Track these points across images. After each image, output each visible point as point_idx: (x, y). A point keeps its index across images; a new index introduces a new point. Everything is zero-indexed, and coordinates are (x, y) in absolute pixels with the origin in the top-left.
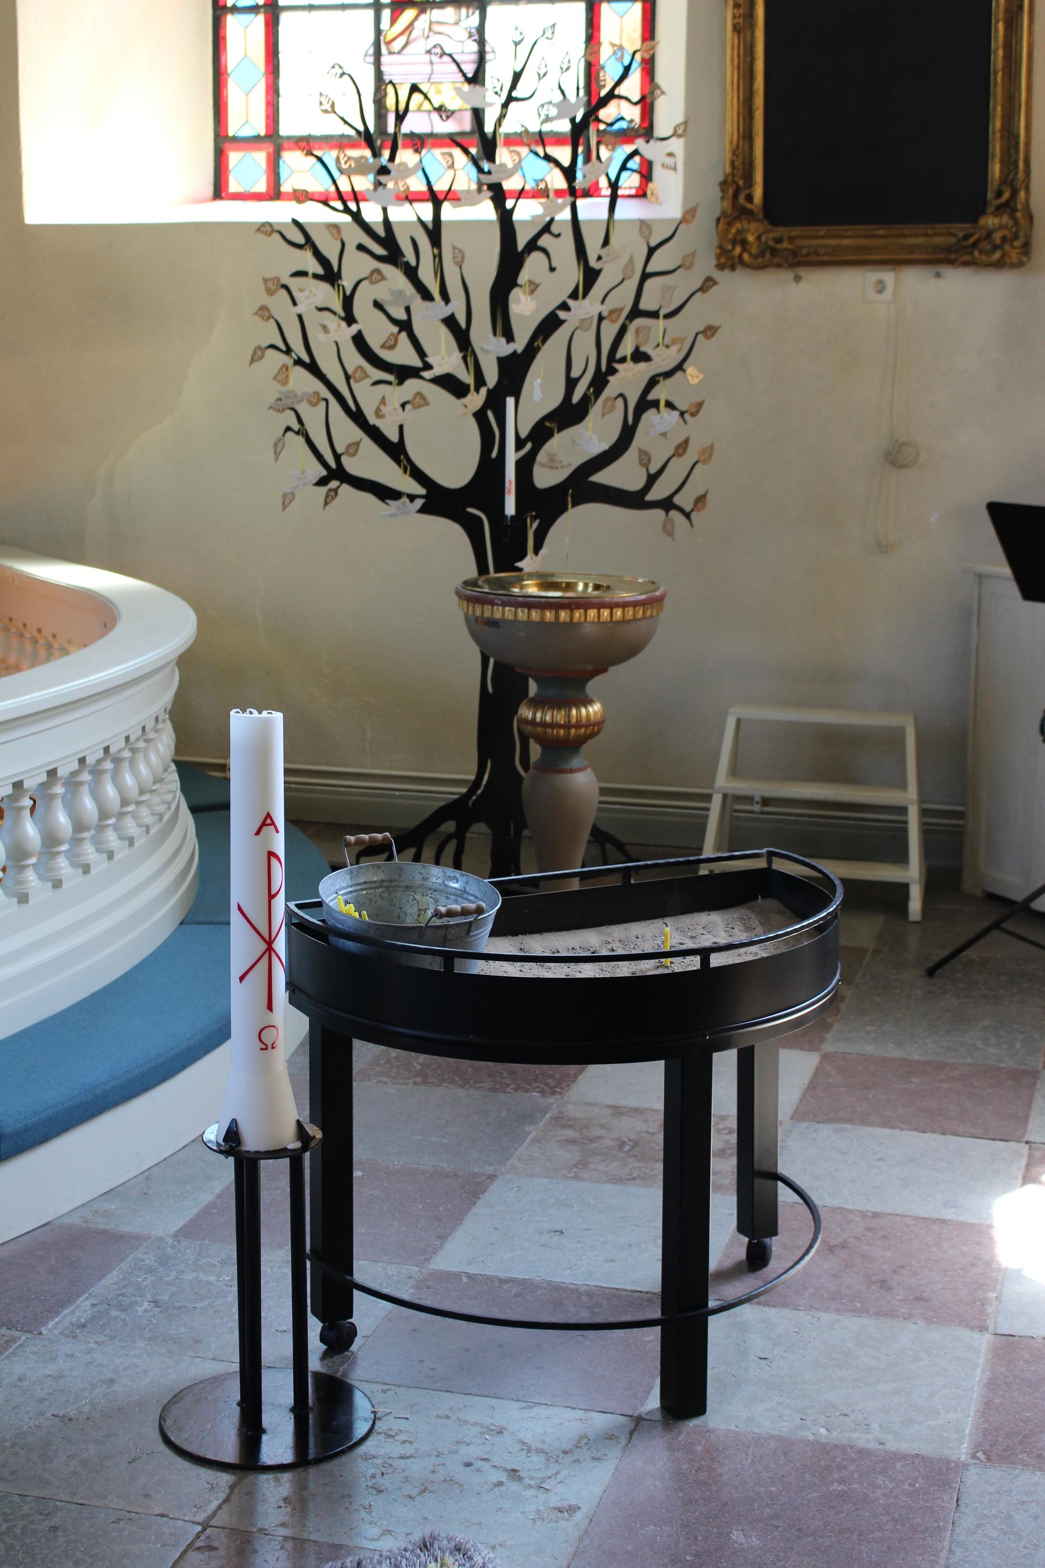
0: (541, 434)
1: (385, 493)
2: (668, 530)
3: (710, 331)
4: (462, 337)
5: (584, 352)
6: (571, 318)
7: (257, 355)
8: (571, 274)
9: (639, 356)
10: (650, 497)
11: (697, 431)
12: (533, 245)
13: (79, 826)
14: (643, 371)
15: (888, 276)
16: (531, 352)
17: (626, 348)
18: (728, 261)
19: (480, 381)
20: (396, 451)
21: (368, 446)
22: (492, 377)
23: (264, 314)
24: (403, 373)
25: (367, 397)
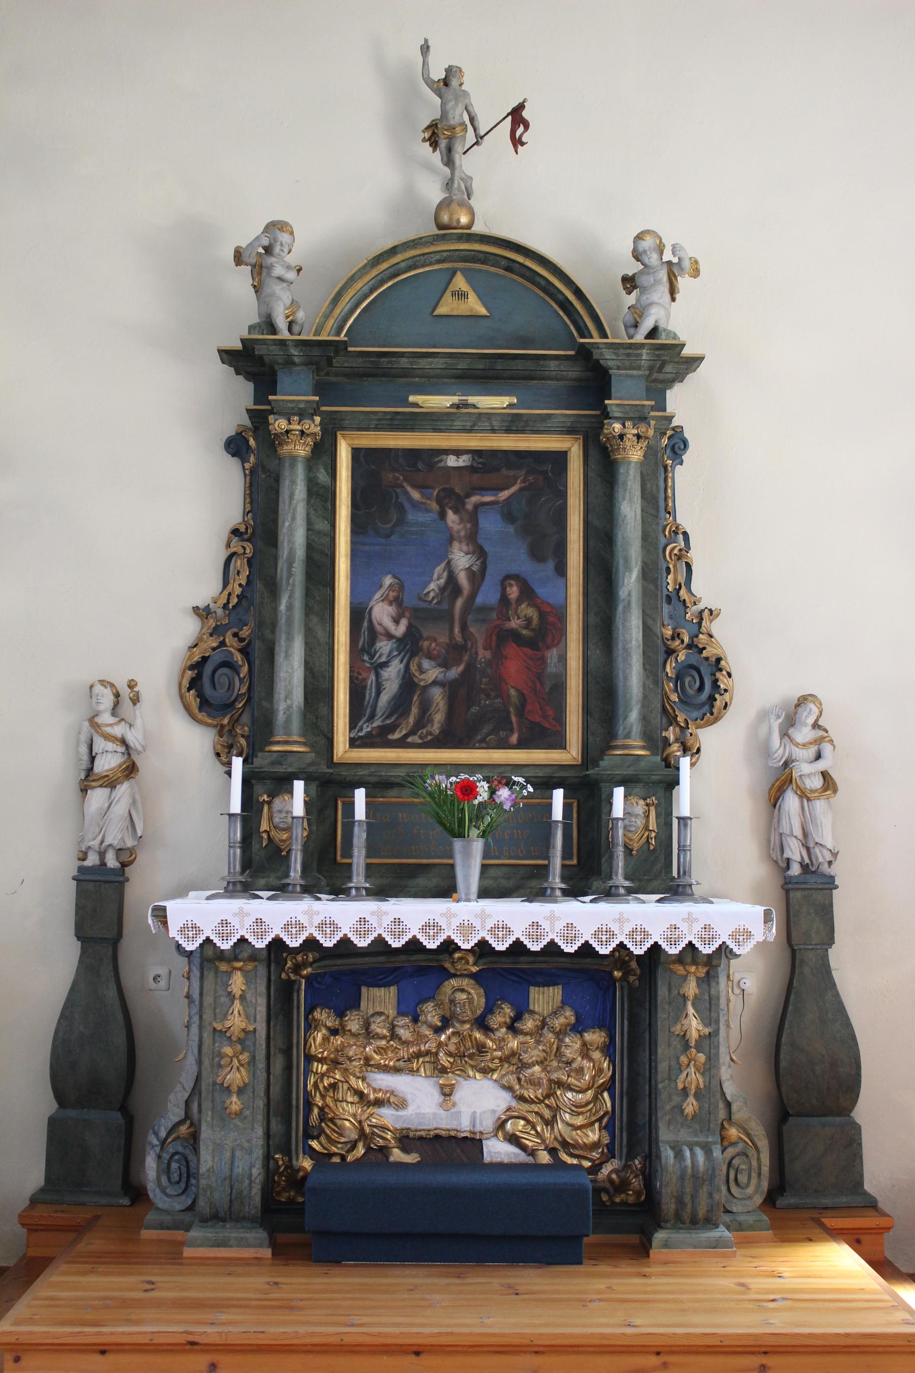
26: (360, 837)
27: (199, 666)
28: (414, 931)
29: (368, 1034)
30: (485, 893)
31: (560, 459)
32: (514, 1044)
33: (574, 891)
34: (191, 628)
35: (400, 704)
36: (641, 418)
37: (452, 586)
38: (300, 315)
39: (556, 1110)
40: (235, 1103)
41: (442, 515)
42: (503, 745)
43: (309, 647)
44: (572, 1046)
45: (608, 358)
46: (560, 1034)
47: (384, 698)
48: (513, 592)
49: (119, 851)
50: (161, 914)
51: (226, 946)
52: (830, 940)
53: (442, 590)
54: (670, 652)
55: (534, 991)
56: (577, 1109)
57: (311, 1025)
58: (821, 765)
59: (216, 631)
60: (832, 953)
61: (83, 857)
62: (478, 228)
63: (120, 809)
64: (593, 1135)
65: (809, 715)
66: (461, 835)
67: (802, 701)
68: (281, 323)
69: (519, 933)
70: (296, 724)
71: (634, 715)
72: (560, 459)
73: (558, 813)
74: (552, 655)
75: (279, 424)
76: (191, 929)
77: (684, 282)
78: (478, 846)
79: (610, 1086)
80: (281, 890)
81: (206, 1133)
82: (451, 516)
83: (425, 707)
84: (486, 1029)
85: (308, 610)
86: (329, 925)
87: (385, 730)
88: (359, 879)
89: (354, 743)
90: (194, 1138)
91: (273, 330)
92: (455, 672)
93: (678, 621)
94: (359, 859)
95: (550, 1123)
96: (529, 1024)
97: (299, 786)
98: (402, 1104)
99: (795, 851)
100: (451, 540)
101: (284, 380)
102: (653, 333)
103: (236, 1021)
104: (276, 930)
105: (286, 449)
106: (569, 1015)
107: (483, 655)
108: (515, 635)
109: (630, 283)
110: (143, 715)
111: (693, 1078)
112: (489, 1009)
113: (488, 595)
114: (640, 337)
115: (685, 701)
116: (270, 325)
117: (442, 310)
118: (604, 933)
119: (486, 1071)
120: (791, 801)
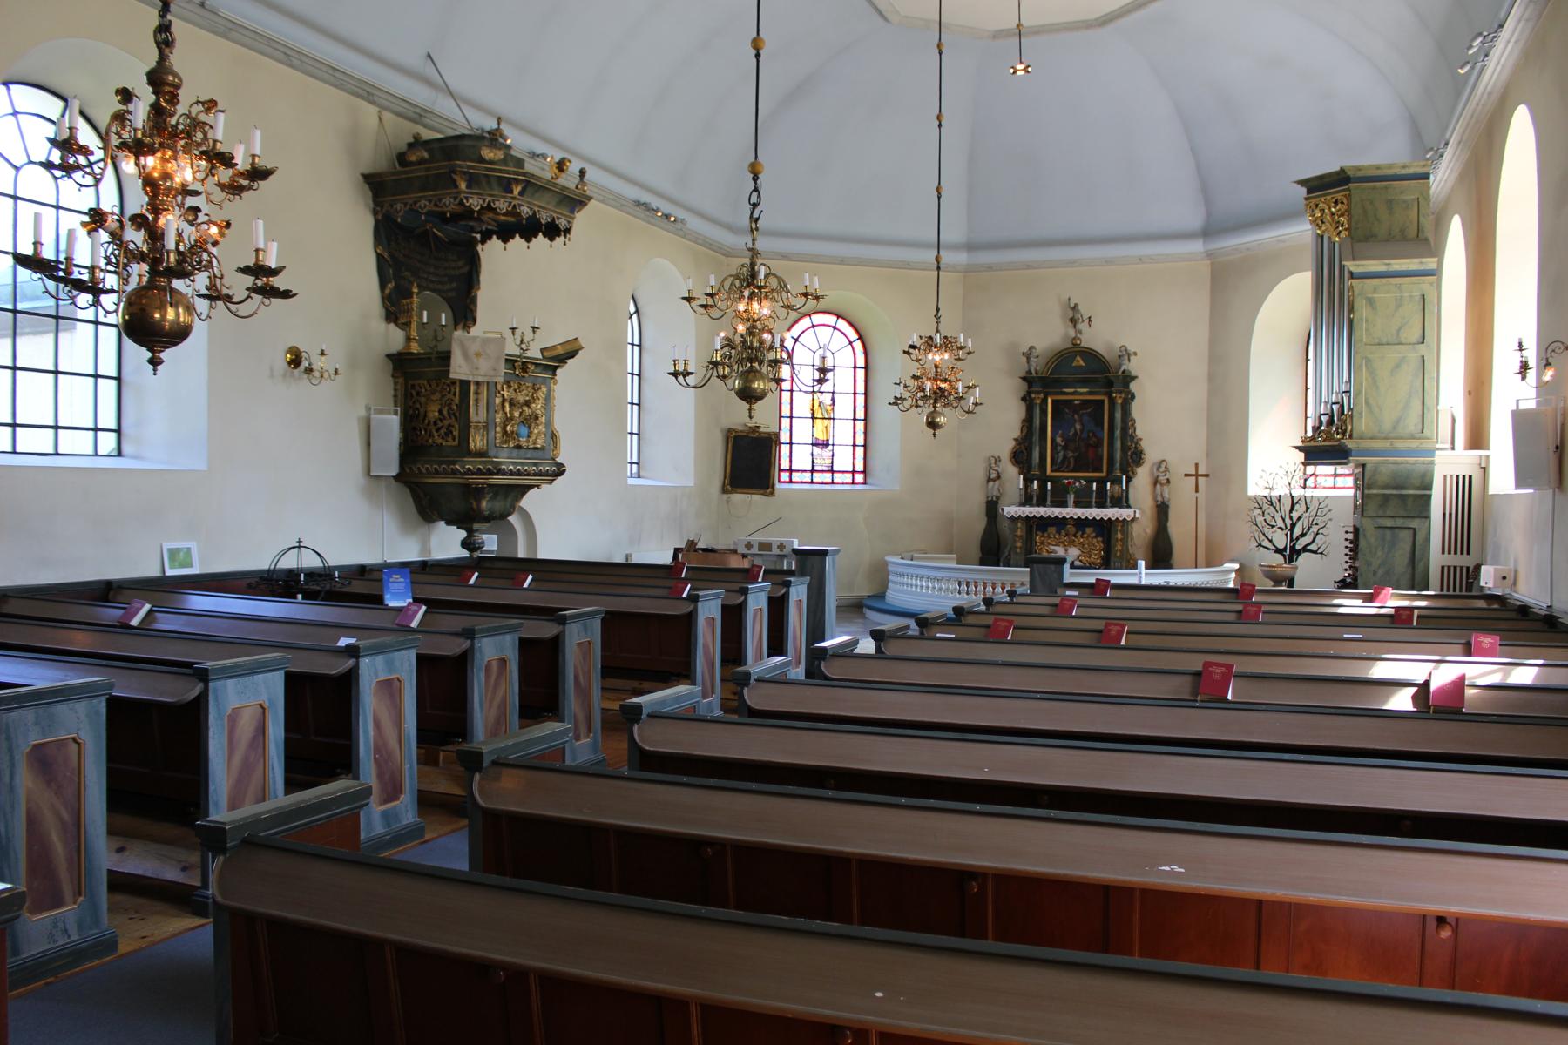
0: (1297, 539)
1: (1268, 549)
2: (1322, 558)
3: (1330, 520)
4: (1284, 520)
5: (1306, 525)
6: (1303, 517)
7: (1247, 522)
8: (1304, 509)
9: (1316, 524)
10: (1319, 551)
12: (1297, 503)
14: (1318, 527)
17: (1314, 523)
19: (1286, 528)
20: (1271, 541)
21: (1266, 540)
22: (1289, 528)
24: (1273, 526)
26: (1049, 494)
27: (1016, 451)
28: (1056, 514)
31: (1103, 401)
32: (1082, 540)
34: (1014, 443)
35: (1063, 462)
36: (1120, 392)
37: (1076, 433)
38: (1038, 368)
40: (1019, 550)
41: (1073, 416)
42: (1088, 472)
43: (1040, 448)
44: (1095, 540)
45: (1112, 378)
46: (1092, 538)
47: (1059, 460)
48: (1091, 435)
50: (1002, 509)
53: (1073, 435)
54: (1130, 449)
56: (1095, 555)
57: (1037, 535)
58: (1167, 477)
59: (1019, 444)
60: (1169, 524)
61: (988, 497)
62: (1082, 345)
63: (996, 486)
64: (1099, 561)
65: (1164, 464)
67: (1163, 461)
68: (1033, 372)
69: (1079, 515)
71: (1118, 465)
72: (1103, 401)
75: (1033, 396)
76: (1009, 513)
77: (1132, 358)
78: (1073, 496)
79: (1103, 550)
80: (1031, 505)
81: (1012, 556)
82: (1076, 416)
83: (1069, 463)
85: (1040, 440)
86: (1038, 512)
87: (1059, 468)
88: (1048, 503)
89: (1052, 471)
90: (1010, 560)
91: (1031, 374)
92: (1076, 454)
93: (1132, 441)
95: (1090, 557)
96: (1085, 536)
97: (1036, 482)
98: (1056, 553)
99: (1159, 499)
100: (1075, 421)
102: (1124, 372)
103: (1019, 533)
104: (1027, 513)
105: (1035, 401)
106: (1094, 534)
109: (1120, 356)
110: (1002, 465)
111: (1119, 547)
112: (1077, 532)
113: (1085, 435)
114: (1120, 373)
115: (1133, 461)
117: (1074, 365)
118: (1098, 515)
119: (1075, 546)
120: (1158, 486)
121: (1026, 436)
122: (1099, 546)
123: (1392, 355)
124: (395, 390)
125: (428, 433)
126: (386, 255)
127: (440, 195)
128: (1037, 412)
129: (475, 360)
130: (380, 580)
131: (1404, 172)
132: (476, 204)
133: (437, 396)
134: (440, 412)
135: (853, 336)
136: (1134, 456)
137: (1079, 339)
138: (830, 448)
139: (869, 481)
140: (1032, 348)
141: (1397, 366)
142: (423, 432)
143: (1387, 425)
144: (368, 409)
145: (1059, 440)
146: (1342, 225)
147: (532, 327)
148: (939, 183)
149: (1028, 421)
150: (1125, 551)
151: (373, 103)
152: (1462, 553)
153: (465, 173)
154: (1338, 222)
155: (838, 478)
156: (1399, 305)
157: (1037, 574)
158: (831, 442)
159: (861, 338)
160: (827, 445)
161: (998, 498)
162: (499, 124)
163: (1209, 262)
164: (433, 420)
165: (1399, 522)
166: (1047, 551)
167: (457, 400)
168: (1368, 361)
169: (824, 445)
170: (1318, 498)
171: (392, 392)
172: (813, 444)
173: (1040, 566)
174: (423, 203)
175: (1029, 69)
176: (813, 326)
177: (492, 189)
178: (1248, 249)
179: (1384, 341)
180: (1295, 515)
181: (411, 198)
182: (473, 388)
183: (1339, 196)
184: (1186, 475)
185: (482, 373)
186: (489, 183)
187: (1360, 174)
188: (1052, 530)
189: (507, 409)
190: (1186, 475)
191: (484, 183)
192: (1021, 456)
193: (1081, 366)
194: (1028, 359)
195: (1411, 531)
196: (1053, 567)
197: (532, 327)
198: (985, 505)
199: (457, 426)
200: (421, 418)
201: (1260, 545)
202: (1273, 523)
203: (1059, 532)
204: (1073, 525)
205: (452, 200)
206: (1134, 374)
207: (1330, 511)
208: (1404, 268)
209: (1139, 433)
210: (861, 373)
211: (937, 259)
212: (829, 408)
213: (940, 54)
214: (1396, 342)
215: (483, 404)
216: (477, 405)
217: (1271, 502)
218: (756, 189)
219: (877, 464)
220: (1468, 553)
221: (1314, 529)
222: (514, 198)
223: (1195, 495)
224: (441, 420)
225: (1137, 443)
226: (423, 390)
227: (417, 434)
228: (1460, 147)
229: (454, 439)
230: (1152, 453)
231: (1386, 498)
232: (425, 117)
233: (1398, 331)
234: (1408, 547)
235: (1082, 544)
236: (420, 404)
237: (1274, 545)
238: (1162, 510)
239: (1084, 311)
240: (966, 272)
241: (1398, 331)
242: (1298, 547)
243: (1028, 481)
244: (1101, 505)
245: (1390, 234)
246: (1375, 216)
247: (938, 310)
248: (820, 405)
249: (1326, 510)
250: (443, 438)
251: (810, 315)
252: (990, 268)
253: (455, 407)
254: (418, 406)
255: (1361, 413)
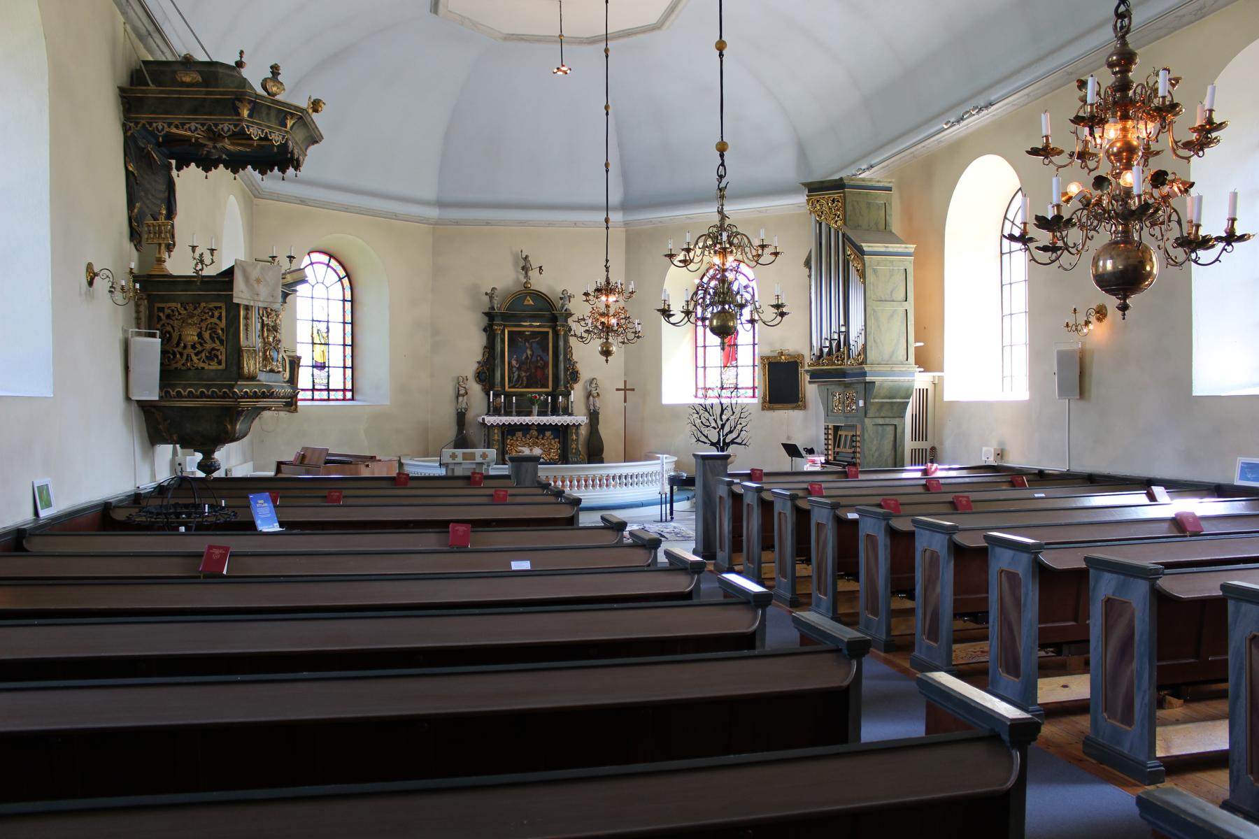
0: (727, 435)
1: (705, 443)
3: (751, 420)
4: (716, 422)
9: (740, 424)
11: (749, 434)
13: (656, 479)
14: (741, 426)
15: (787, 411)
16: (725, 423)
18: (763, 409)
20: (707, 437)
22: (720, 427)
23: (689, 418)
24: (708, 426)
25: (702, 429)
27: (479, 373)
29: (517, 440)
30: (538, 415)
31: (548, 332)
33: (553, 415)
34: (476, 366)
35: (517, 381)
36: (563, 326)
37: (527, 358)
39: (550, 453)
42: (537, 388)
43: (501, 370)
44: (553, 442)
45: (558, 315)
47: (514, 379)
48: (539, 358)
49: (465, 409)
51: (495, 424)
52: (598, 424)
55: (546, 433)
57: (507, 439)
58: (597, 391)
59: (482, 366)
62: (531, 288)
65: (595, 381)
66: (534, 405)
67: (593, 379)
70: (499, 384)
71: (562, 383)
72: (548, 332)
73: (550, 401)
74: (546, 371)
75: (496, 327)
76: (489, 421)
77: (571, 299)
78: (537, 407)
80: (500, 415)
82: (527, 344)
84: (538, 439)
87: (515, 385)
88: (514, 413)
89: (509, 388)
91: (494, 310)
92: (528, 374)
94: (514, 409)
97: (503, 396)
99: (592, 407)
100: (527, 348)
101: (496, 319)
102: (566, 310)
103: (496, 437)
104: (504, 422)
107: (533, 371)
108: (539, 367)
109: (561, 299)
111: (574, 446)
112: (538, 436)
113: (534, 359)
115: (571, 379)
116: (493, 308)
117: (525, 303)
119: (538, 447)
120: (591, 398)
121: (487, 359)
122: (557, 445)
123: (889, 307)
124: (138, 312)
125: (185, 357)
126: (136, 173)
127: (152, 118)
128: (498, 340)
129: (256, 285)
130: (248, 507)
131: (878, 184)
132: (255, 134)
133: (195, 320)
134: (200, 335)
135: (342, 273)
136: (573, 376)
137: (530, 283)
138: (327, 369)
139: (356, 397)
140: (493, 289)
141: (892, 316)
142: (178, 356)
143: (886, 357)
144: (125, 331)
145: (514, 363)
146: (838, 217)
147: (288, 257)
148: (607, 160)
149: (490, 348)
150: (577, 449)
151: (124, 13)
152: (919, 440)
153: (250, 101)
154: (836, 215)
155: (333, 395)
156: (891, 275)
157: (708, 467)
158: (327, 365)
159: (348, 275)
160: (324, 367)
161: (466, 410)
162: (241, 57)
163: (624, 229)
164: (189, 344)
165: (887, 421)
166: (516, 452)
167: (223, 324)
168: (875, 311)
169: (322, 367)
170: (741, 405)
171: (134, 315)
172: (313, 367)
173: (711, 461)
174: (193, 125)
175: (555, 70)
176: (312, 264)
177: (269, 121)
178: (660, 222)
179: (883, 298)
180: (724, 417)
181: (178, 119)
182: (242, 313)
183: (836, 196)
184: (617, 390)
185: (262, 299)
186: (268, 114)
187: (852, 183)
188: (519, 434)
189: (266, 334)
190: (617, 390)
191: (264, 114)
192: (485, 375)
193: (531, 305)
194: (491, 298)
195: (893, 427)
196: (719, 462)
197: (288, 257)
198: (456, 416)
199: (223, 349)
200: (175, 341)
201: (698, 440)
202: (708, 424)
203: (524, 435)
204: (536, 430)
205: (232, 127)
206: (573, 312)
207: (750, 414)
208: (895, 250)
209: (575, 358)
210: (348, 305)
211: (607, 220)
212: (325, 335)
213: (607, 57)
214: (891, 299)
215: (256, 325)
216: (247, 330)
217: (706, 408)
218: (722, 164)
219: (363, 383)
220: (926, 440)
221: (739, 427)
222: (287, 132)
223: (623, 404)
224: (201, 344)
225: (574, 365)
226: (177, 314)
227: (169, 357)
228: (881, 171)
229: (220, 363)
230: (585, 374)
231: (883, 404)
232: (152, 37)
233: (892, 292)
234: (891, 438)
235: (544, 445)
236: (173, 327)
237: (709, 440)
238: (594, 416)
239: (535, 263)
240: (436, 224)
241: (892, 292)
242: (727, 441)
243: (497, 395)
244: (555, 412)
245: (869, 226)
246: (860, 213)
247: (607, 261)
248: (318, 333)
249: (747, 413)
250: (204, 362)
251: (309, 254)
252: (457, 223)
253: (220, 332)
254: (169, 328)
255: (871, 347)
